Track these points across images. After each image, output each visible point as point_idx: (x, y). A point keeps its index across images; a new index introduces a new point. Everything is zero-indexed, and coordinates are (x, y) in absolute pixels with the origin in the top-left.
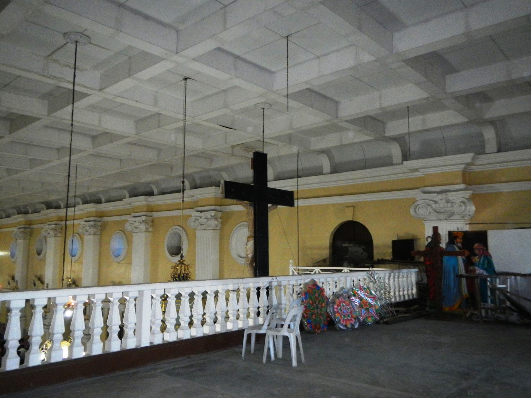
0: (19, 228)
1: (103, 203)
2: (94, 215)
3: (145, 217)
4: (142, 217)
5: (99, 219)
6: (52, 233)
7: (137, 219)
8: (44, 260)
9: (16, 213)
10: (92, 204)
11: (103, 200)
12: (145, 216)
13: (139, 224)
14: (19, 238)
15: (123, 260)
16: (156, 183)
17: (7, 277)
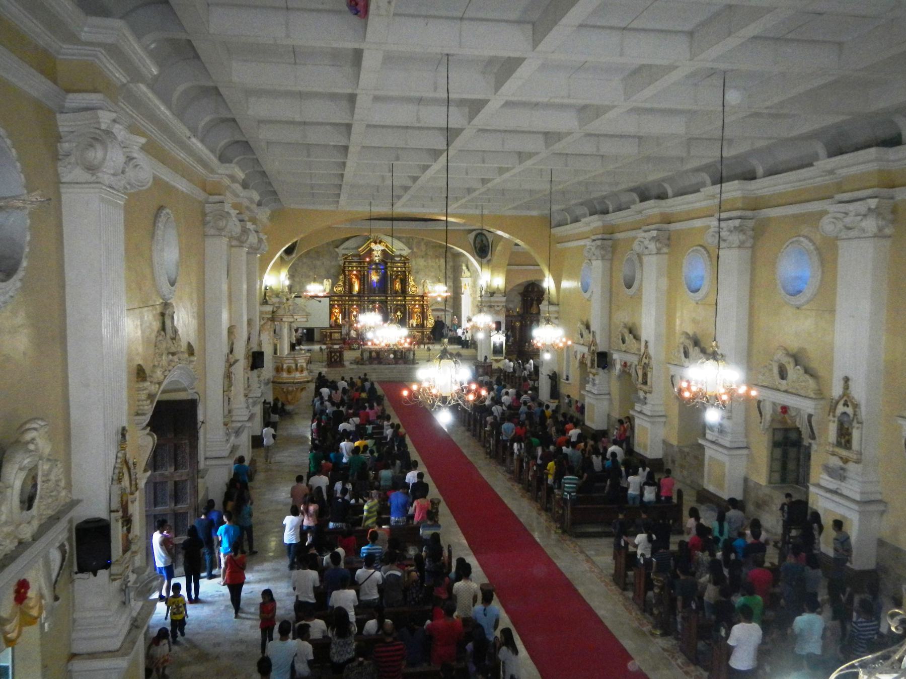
0: (594, 240)
1: (760, 178)
2: (739, 205)
3: (876, 200)
4: (869, 201)
5: (749, 213)
6: (652, 246)
7: (851, 207)
8: (638, 297)
9: (588, 213)
10: (736, 182)
11: (760, 171)
13: (859, 218)
14: (594, 258)
15: (808, 302)
17: (579, 325)
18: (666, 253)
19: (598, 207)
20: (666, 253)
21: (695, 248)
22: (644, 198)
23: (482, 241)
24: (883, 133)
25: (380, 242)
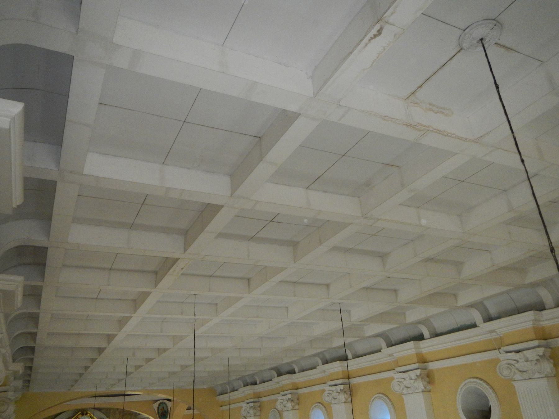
0: (248, 403)
2: (341, 376)
6: (289, 405)
7: (405, 375)
9: (242, 385)
10: (338, 362)
12: (418, 369)
13: (412, 381)
14: (249, 415)
16: (425, 322)
18: (298, 409)
19: (249, 381)
20: (298, 409)
21: (316, 404)
22: (280, 374)
23: (163, 408)
24: (413, 332)
25: (87, 414)
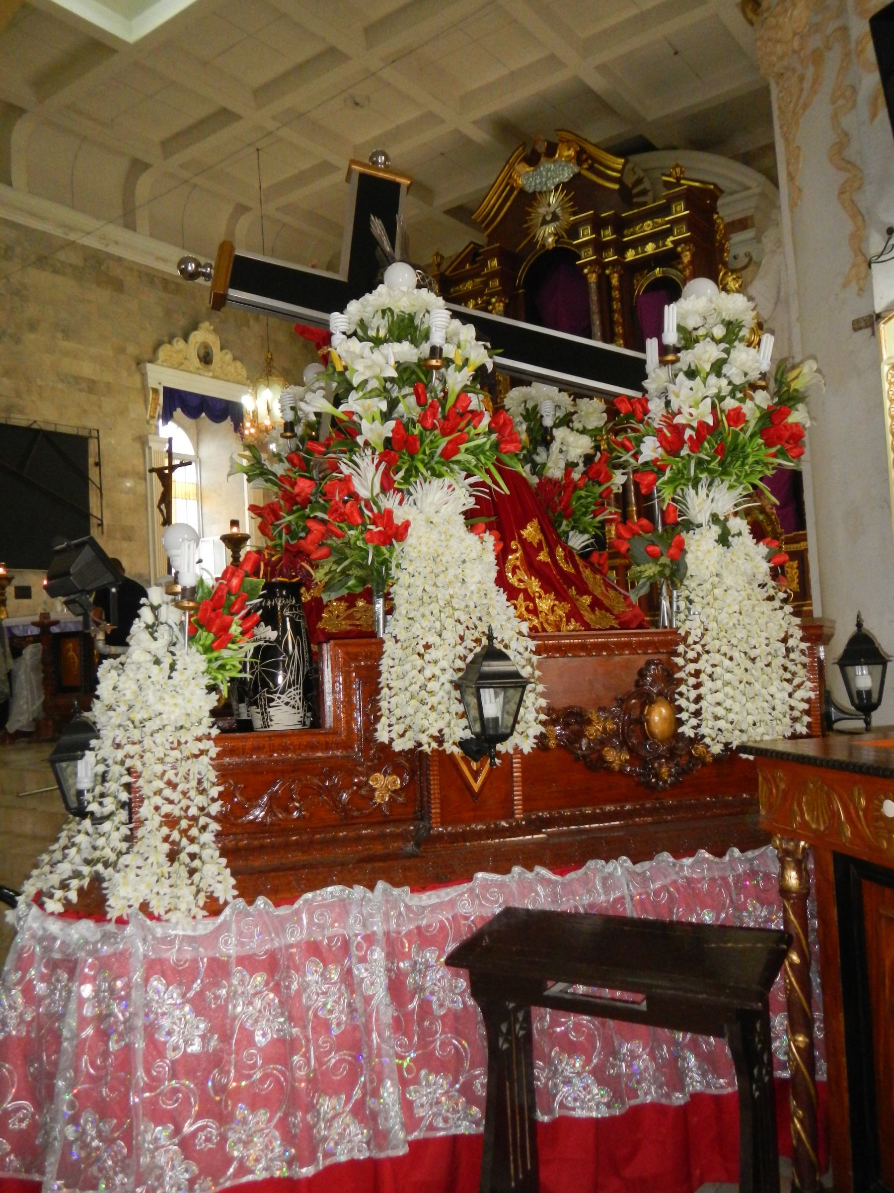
25: (551, 151)
